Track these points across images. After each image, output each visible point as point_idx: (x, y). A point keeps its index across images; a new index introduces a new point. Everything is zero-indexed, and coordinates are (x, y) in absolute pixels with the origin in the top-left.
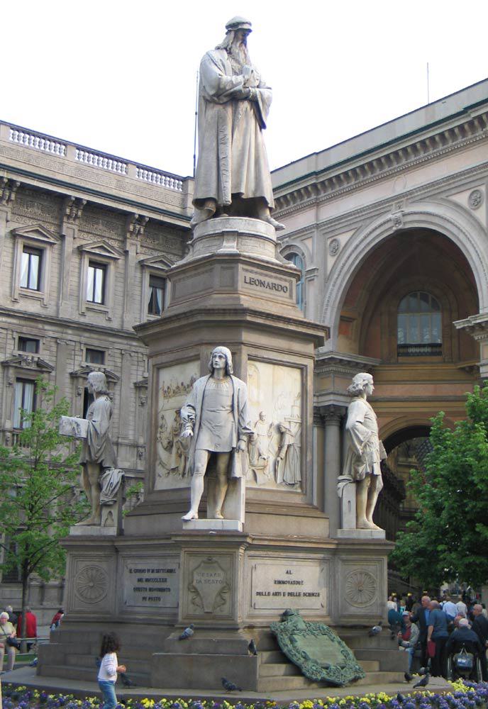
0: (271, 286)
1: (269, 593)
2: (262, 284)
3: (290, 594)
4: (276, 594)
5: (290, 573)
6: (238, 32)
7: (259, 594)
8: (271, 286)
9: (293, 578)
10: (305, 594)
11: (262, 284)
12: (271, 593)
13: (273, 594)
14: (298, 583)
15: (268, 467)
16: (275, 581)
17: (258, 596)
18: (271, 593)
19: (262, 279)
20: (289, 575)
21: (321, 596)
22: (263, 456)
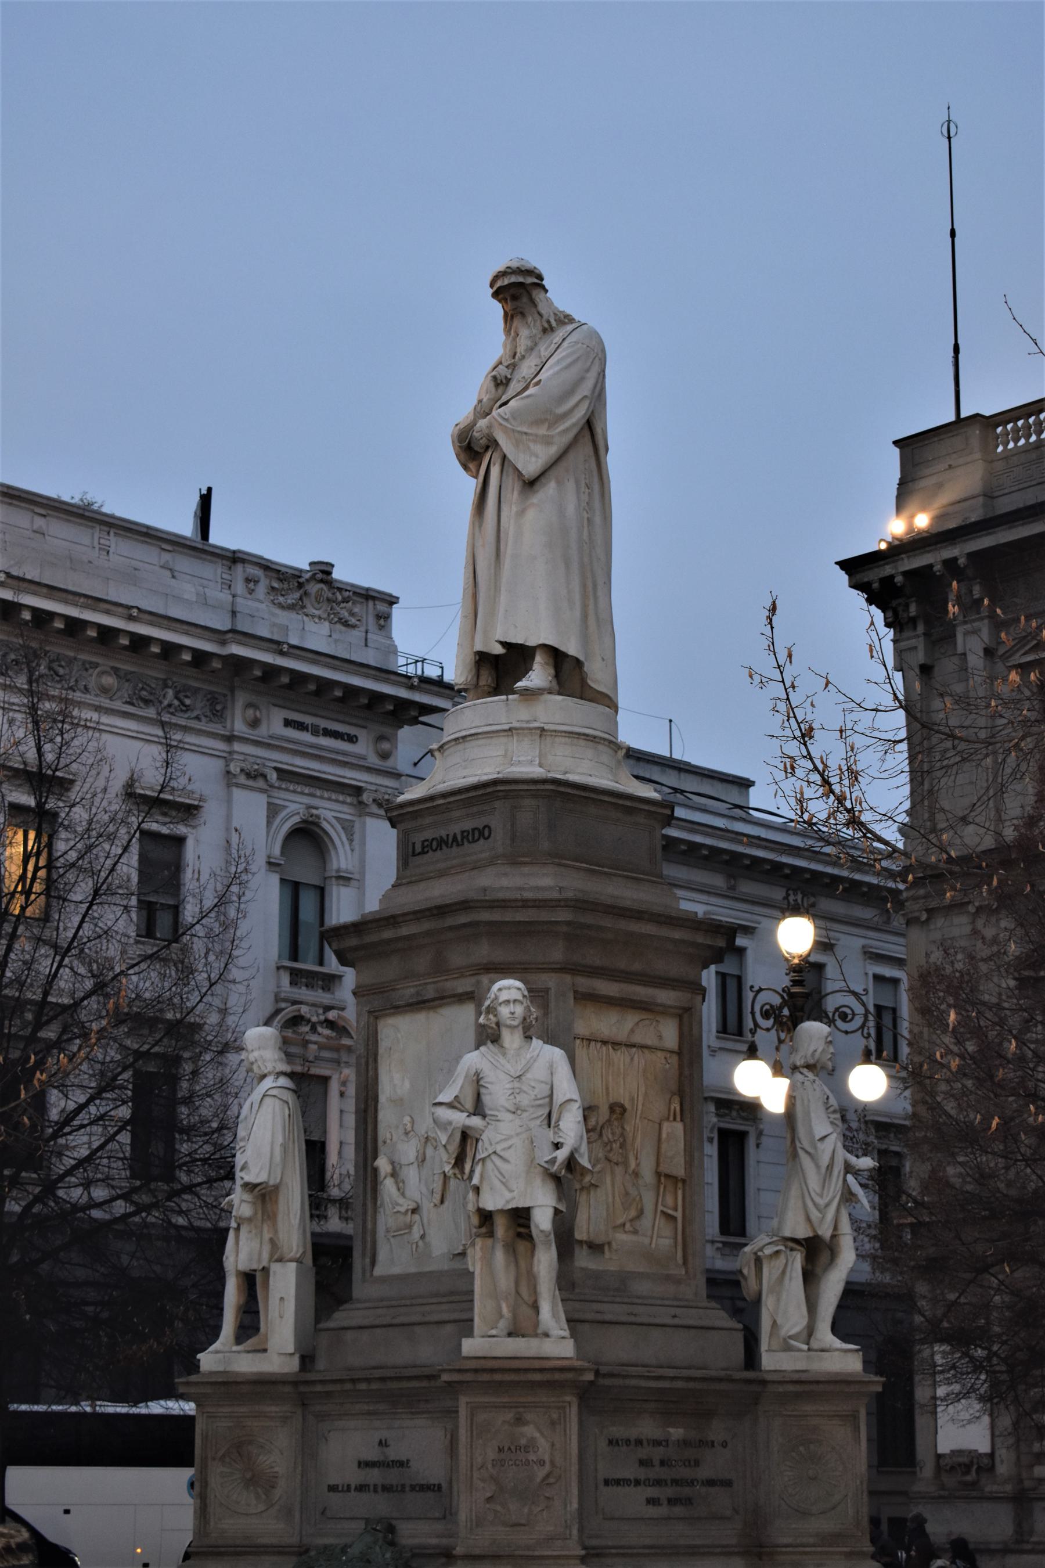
0: (459, 839)
1: (349, 1486)
2: (442, 843)
3: (387, 1489)
4: (361, 1488)
5: (387, 1446)
6: (518, 292)
7: (333, 1488)
8: (459, 839)
9: (392, 1454)
10: (413, 1488)
11: (442, 843)
12: (353, 1487)
13: (356, 1489)
14: (402, 1464)
15: (415, 1228)
16: (360, 1463)
17: (331, 1494)
18: (353, 1487)
19: (443, 833)
20: (386, 1450)
21: (443, 1489)
22: (398, 1208)
